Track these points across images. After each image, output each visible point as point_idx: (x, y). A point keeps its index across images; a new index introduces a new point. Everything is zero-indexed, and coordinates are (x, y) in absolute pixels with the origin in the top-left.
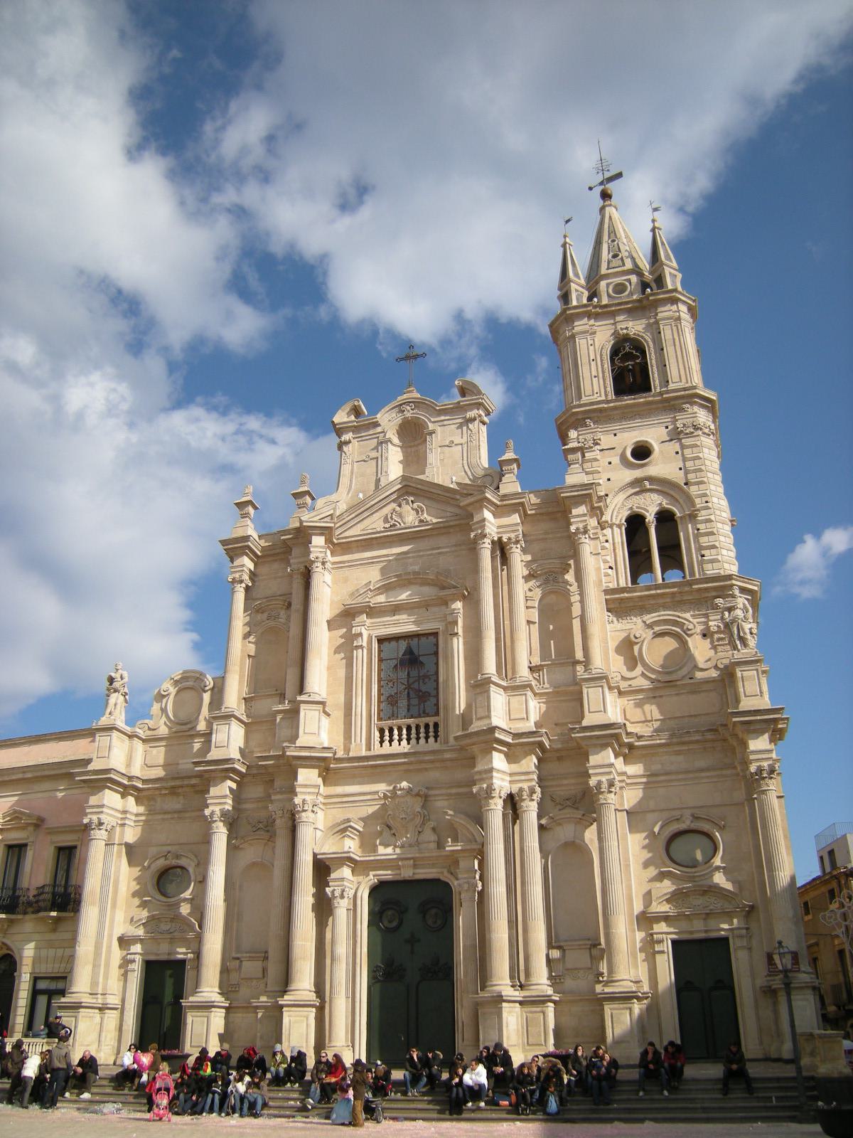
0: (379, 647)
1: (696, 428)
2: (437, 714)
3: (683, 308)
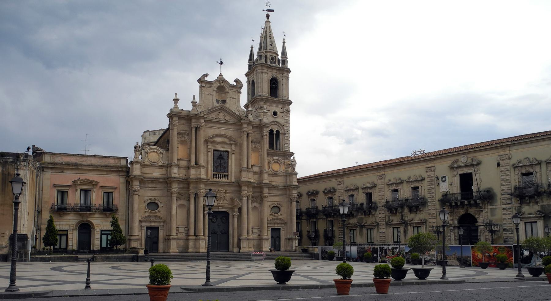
2: (228, 173)
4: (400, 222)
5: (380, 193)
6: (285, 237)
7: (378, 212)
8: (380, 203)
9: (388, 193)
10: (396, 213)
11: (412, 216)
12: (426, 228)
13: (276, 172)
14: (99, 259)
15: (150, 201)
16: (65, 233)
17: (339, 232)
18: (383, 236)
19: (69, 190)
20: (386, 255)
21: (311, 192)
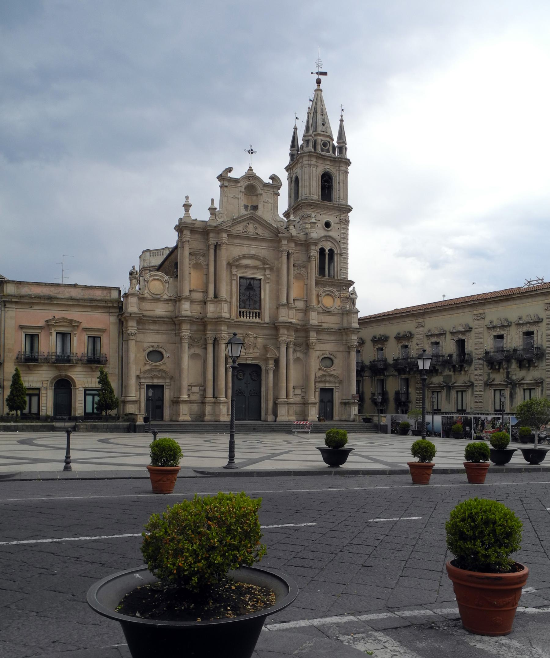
2: (260, 309)
4: (504, 381)
5: (477, 340)
6: (340, 401)
7: (473, 367)
8: (476, 354)
9: (489, 340)
10: (499, 369)
11: (523, 373)
12: (542, 391)
13: (328, 308)
14: (83, 428)
15: (151, 349)
16: (37, 392)
17: (417, 394)
18: (480, 402)
19: (40, 333)
20: (483, 429)
21: (377, 337)
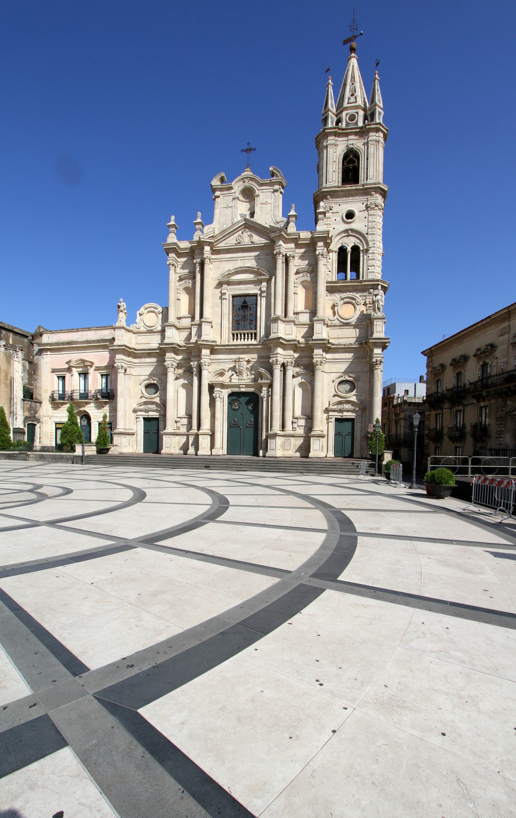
0: (233, 299)
1: (377, 206)
2: (256, 329)
3: (381, 135)
17: (497, 427)
21: (457, 360)
